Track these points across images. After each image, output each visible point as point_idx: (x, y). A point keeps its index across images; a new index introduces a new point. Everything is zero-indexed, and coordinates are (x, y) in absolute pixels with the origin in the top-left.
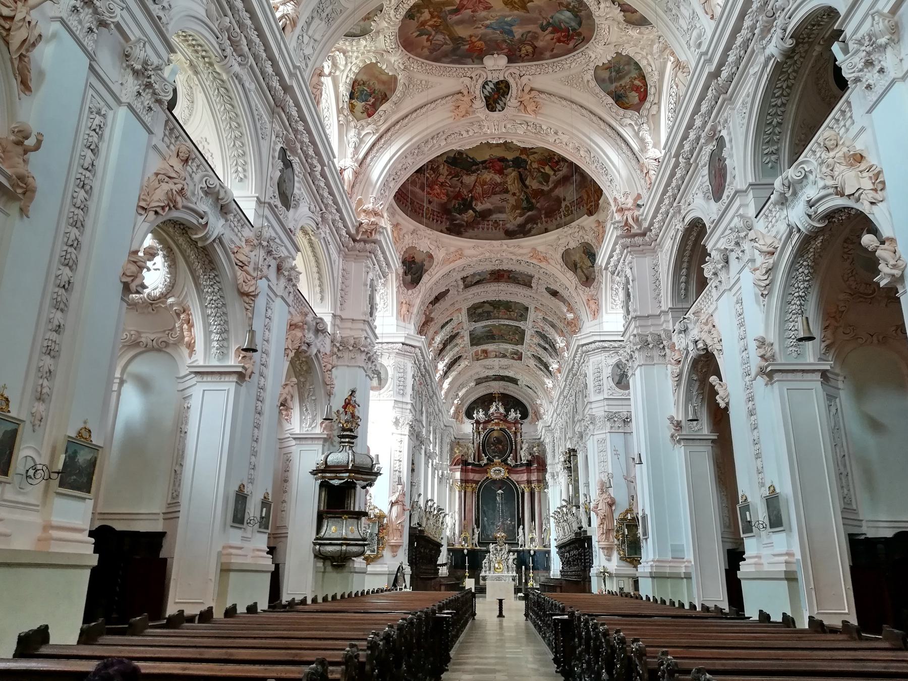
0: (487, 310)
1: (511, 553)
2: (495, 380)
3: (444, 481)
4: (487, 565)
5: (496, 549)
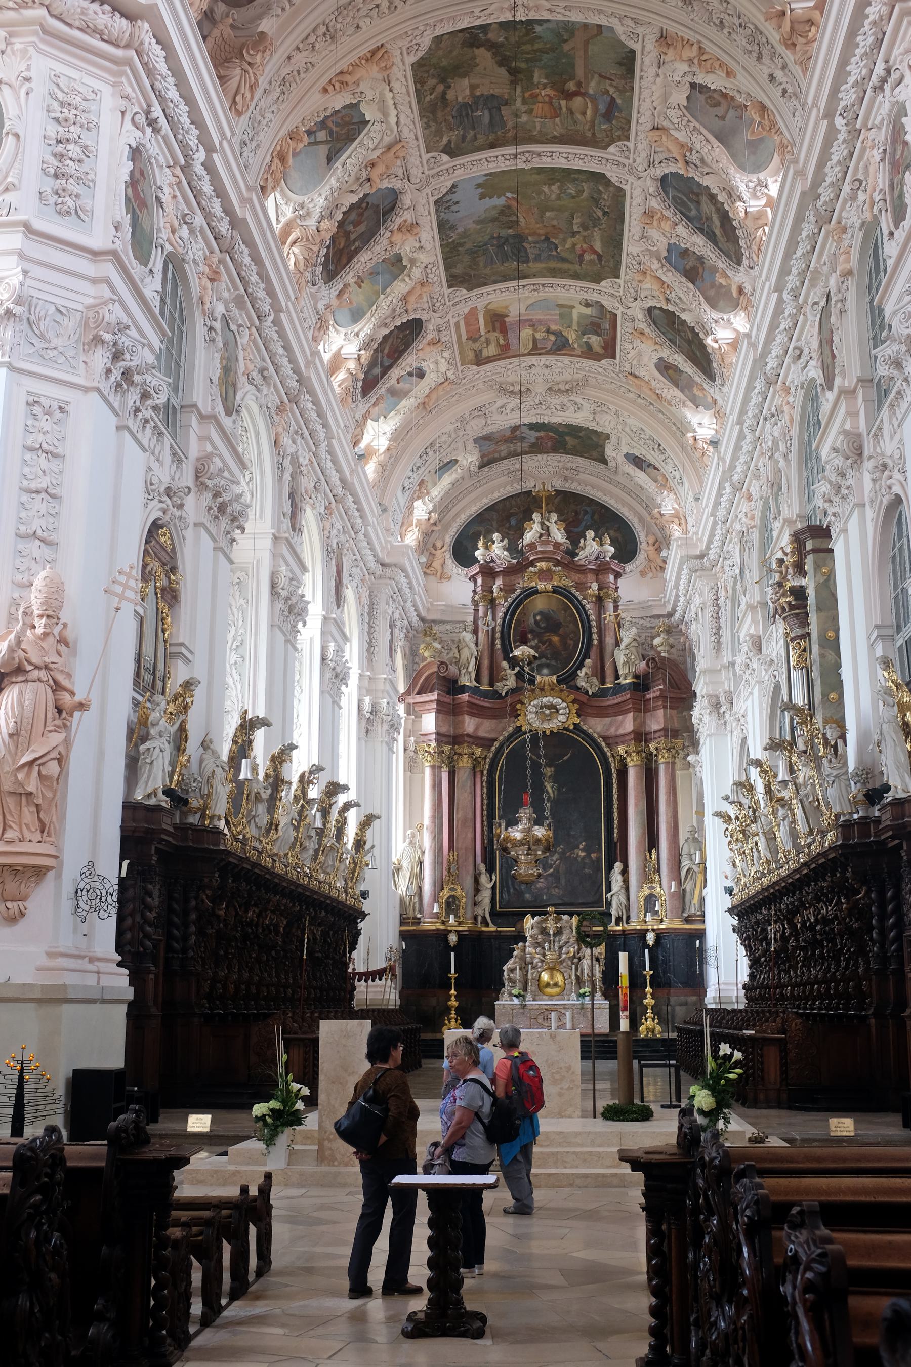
0: (484, 90)
2: (537, 448)
3: (381, 730)
4: (517, 975)
5: (544, 931)
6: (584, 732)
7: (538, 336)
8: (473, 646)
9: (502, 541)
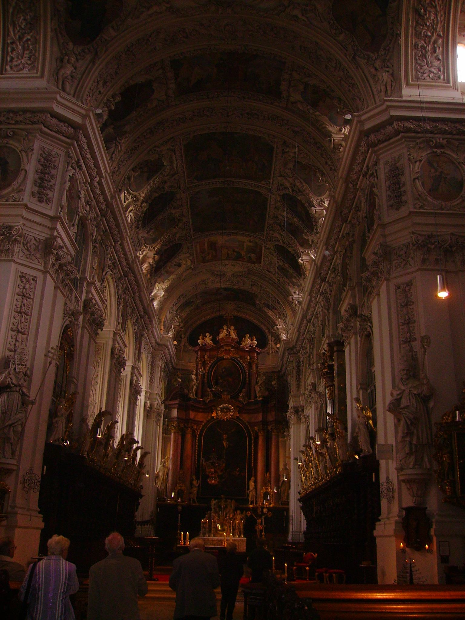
1: (238, 512)
3: (154, 416)
6: (241, 420)
7: (229, 252)
8: (195, 381)
9: (210, 337)
